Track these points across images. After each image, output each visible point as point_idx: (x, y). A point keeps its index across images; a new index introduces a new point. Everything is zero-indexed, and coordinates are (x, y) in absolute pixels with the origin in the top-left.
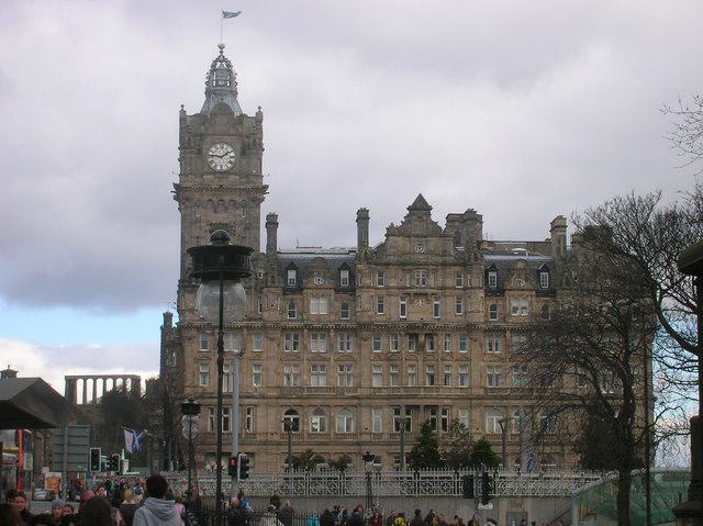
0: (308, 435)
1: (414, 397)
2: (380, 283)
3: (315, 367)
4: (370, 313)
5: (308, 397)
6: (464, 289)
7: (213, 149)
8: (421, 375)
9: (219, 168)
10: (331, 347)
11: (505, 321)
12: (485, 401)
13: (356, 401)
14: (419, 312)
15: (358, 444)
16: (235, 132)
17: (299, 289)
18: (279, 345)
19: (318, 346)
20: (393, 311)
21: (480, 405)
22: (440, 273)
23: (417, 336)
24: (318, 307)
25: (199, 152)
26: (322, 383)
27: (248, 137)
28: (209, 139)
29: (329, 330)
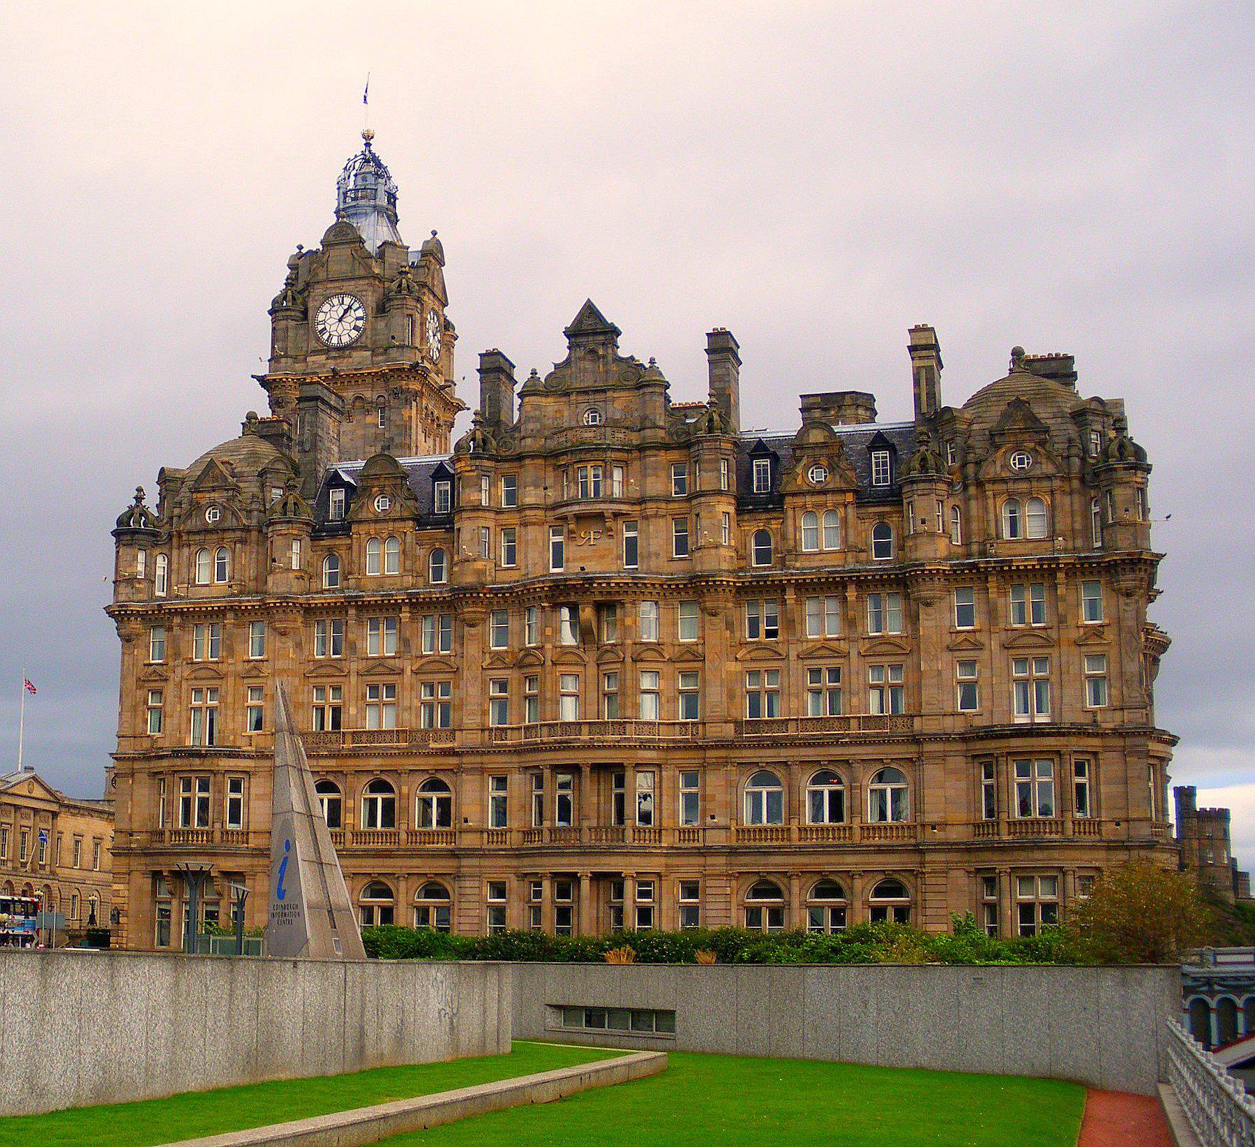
0: (356, 834)
1: (565, 746)
2: (511, 497)
3: (374, 689)
4: (479, 565)
5: (354, 754)
6: (688, 500)
7: (326, 308)
8: (592, 695)
9: (335, 341)
10: (405, 643)
11: (784, 566)
12: (737, 753)
13: (453, 761)
14: (594, 557)
15: (454, 854)
16: (362, 273)
17: (344, 528)
18: (299, 645)
19: (378, 643)
20: (538, 557)
21: (725, 762)
22: (637, 464)
24: (382, 562)
25: (305, 313)
26: (388, 724)
27: (406, 285)
28: (318, 291)
29: (397, 607)
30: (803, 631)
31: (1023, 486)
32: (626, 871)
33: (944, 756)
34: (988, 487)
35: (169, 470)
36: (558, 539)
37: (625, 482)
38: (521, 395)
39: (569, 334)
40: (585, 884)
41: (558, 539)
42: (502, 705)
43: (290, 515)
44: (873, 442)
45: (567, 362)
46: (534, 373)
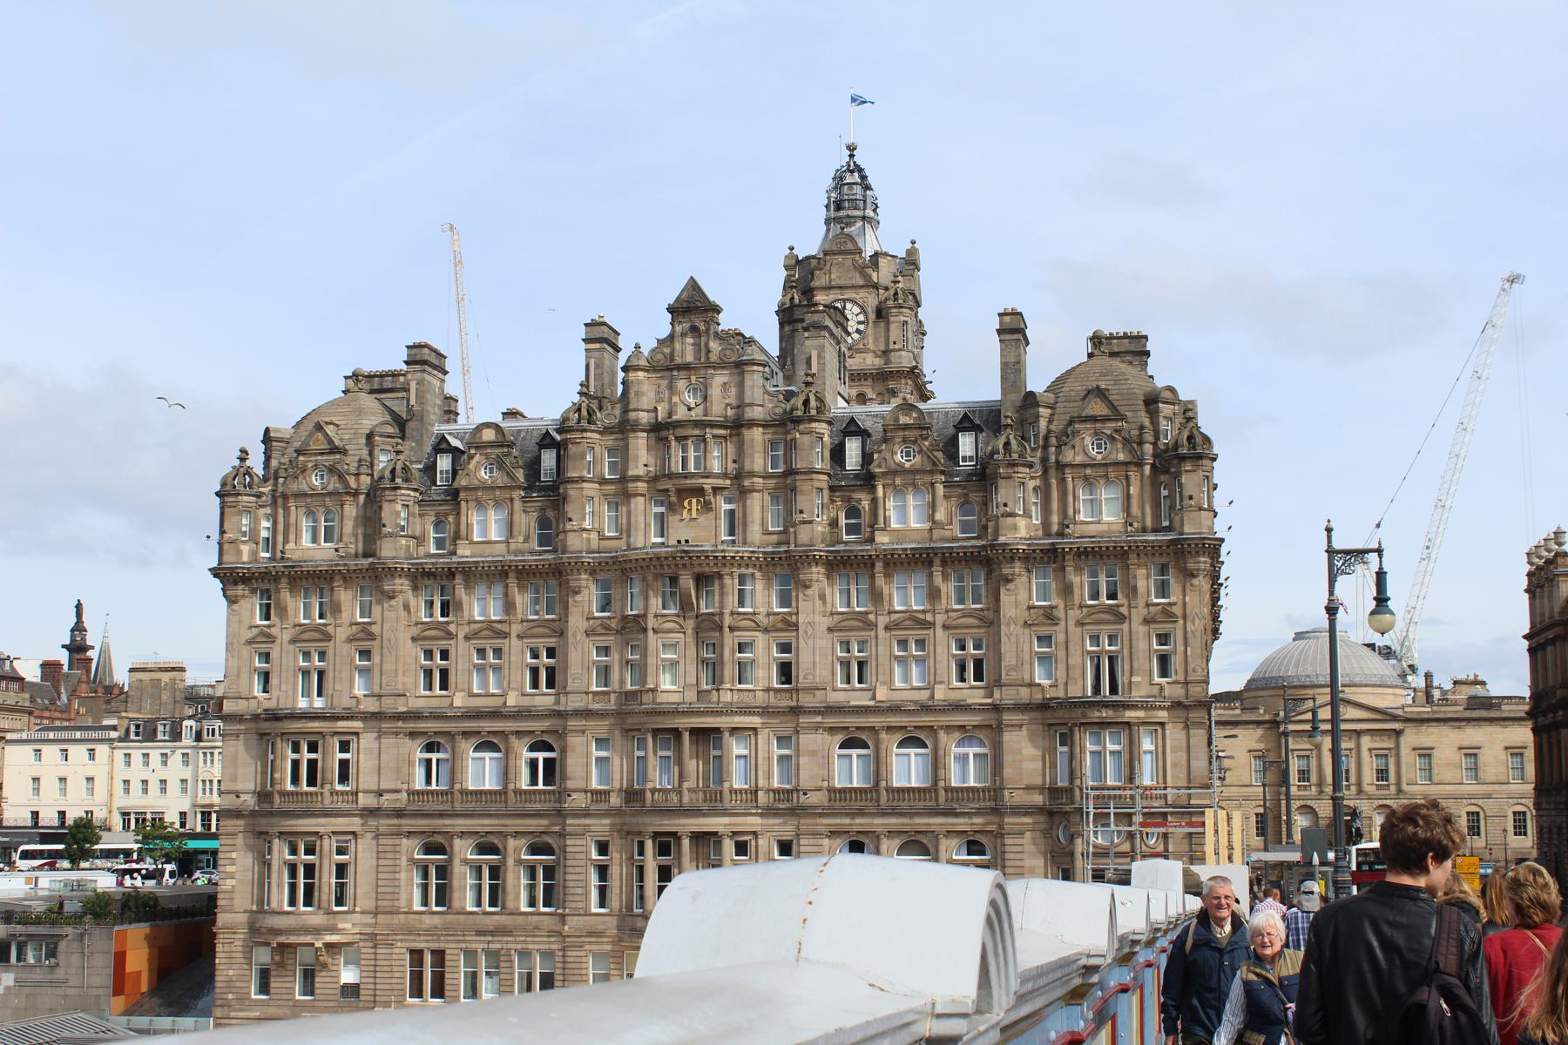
17: (453, 495)
23: (674, 580)
30: (891, 604)
31: (1101, 471)
32: (720, 829)
33: (1021, 726)
34: (1068, 470)
35: (278, 430)
36: (662, 509)
37: (724, 457)
38: (625, 369)
39: (671, 310)
40: (686, 843)
41: (662, 509)
42: (605, 672)
43: (398, 480)
44: (961, 422)
45: (671, 337)
46: (637, 347)
